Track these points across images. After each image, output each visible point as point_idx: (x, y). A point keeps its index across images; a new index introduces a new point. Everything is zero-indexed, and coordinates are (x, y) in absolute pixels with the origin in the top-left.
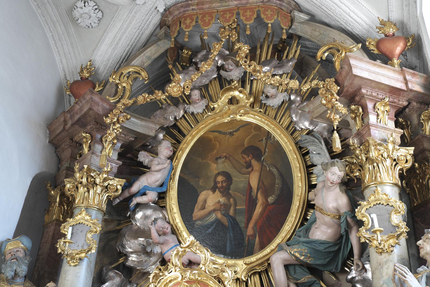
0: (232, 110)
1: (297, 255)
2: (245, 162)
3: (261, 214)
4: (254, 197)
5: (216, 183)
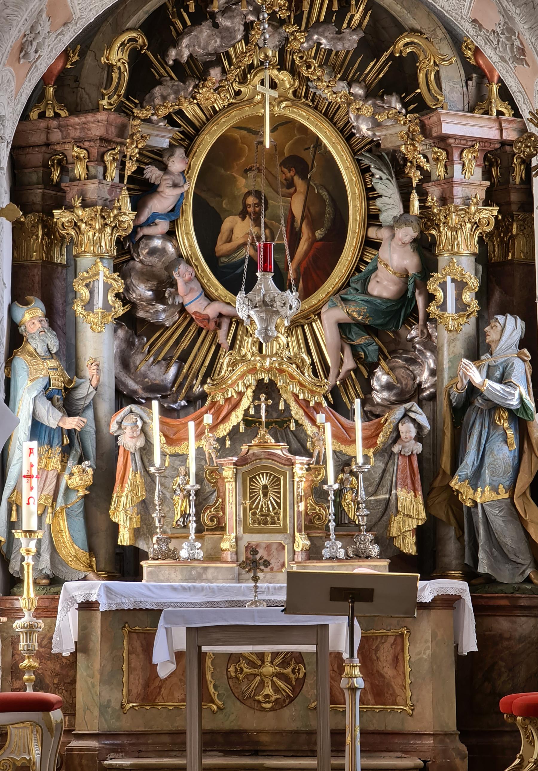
0: (268, 98)
1: (355, 315)
2: (285, 179)
3: (306, 253)
4: (297, 229)
5: (245, 206)
